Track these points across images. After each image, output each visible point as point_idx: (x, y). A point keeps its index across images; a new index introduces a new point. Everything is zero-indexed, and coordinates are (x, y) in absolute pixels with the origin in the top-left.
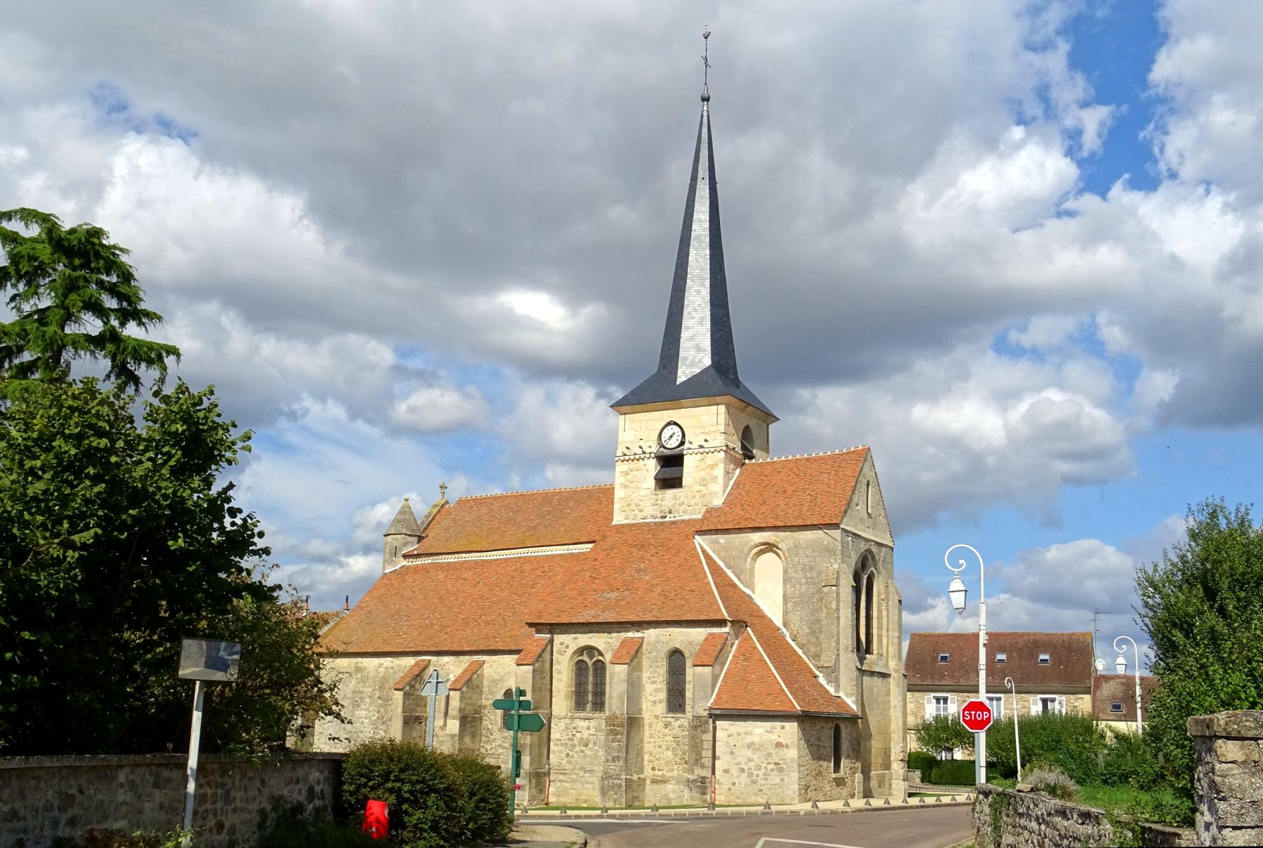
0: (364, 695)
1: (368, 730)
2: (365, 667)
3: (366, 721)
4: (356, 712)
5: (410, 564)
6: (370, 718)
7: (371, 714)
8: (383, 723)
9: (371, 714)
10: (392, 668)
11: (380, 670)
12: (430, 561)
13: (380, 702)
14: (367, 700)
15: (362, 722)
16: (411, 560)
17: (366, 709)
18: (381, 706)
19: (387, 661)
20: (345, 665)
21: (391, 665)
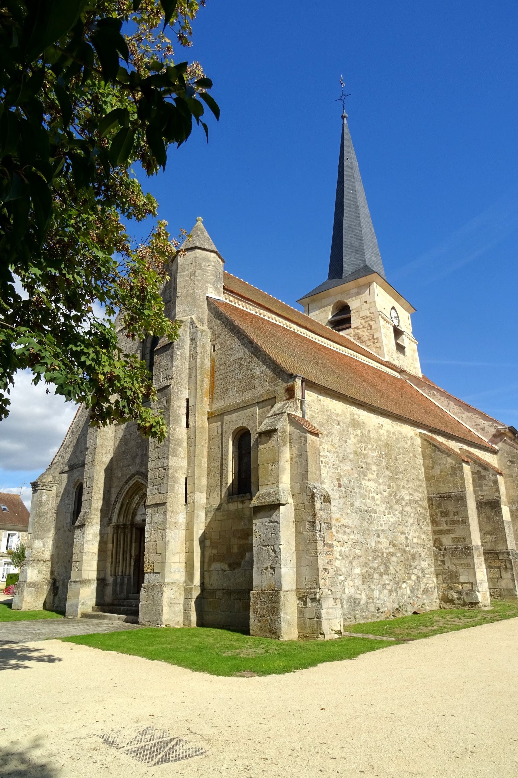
0: (369, 460)
1: (382, 510)
2: (364, 423)
3: (377, 497)
4: (363, 482)
5: (227, 301)
6: (381, 494)
7: (381, 487)
8: (397, 502)
9: (381, 487)
10: (394, 433)
11: (381, 431)
12: (253, 312)
13: (388, 473)
14: (374, 468)
15: (373, 497)
16: (232, 298)
17: (375, 481)
18: (390, 478)
19: (387, 423)
20: (339, 411)
21: (392, 430)
